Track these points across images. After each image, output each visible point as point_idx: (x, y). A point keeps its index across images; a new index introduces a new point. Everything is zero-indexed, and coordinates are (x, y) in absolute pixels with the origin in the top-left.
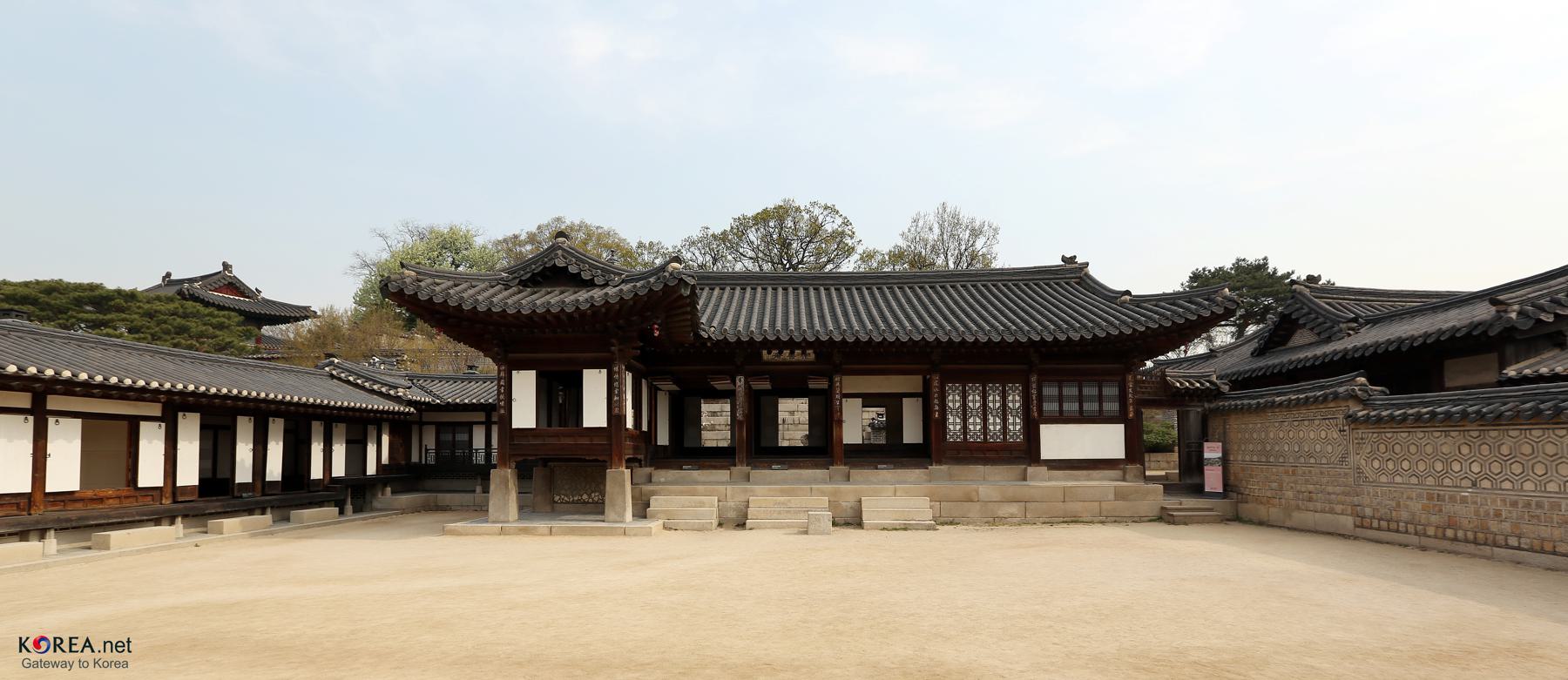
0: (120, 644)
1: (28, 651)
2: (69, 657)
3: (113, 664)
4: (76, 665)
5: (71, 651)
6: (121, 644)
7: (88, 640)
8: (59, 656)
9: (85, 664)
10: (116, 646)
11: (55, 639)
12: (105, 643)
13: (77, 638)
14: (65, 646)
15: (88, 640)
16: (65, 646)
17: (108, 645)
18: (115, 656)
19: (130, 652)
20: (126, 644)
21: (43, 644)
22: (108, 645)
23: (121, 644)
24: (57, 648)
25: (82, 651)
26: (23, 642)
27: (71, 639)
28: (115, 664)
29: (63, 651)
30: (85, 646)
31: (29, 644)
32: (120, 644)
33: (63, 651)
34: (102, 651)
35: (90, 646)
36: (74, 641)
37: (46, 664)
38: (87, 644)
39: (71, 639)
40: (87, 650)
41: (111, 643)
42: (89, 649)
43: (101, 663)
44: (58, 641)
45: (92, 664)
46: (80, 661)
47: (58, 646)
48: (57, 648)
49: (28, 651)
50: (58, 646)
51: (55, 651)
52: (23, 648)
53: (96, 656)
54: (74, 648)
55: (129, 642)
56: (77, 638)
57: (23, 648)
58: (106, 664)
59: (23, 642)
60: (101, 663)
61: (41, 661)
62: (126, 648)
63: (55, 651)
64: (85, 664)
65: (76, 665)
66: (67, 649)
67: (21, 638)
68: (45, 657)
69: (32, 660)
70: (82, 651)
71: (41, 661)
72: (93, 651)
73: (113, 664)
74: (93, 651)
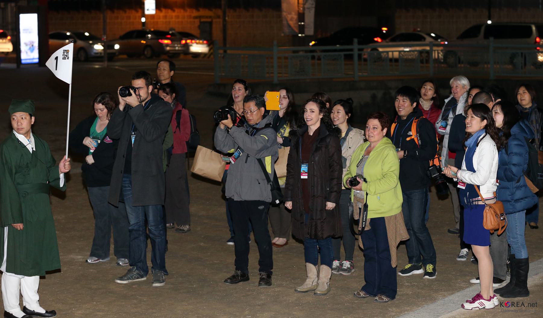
5: (517, 306)
7: (523, 303)
11: (512, 302)
12: (528, 304)
13: (519, 302)
14: (515, 305)
15: (523, 303)
16: (515, 305)
17: (529, 305)
22: (529, 305)
26: (502, 303)
29: (515, 307)
30: (522, 305)
31: (503, 304)
34: (528, 306)
35: (524, 305)
36: (518, 303)
37: (509, 311)
38: (523, 304)
39: (517, 302)
40: (523, 306)
41: (531, 304)
44: (513, 303)
47: (513, 305)
49: (503, 306)
51: (512, 307)
52: (501, 305)
54: (518, 305)
56: (519, 302)
57: (501, 305)
59: (502, 303)
63: (512, 307)
66: (516, 306)
67: (501, 302)
72: (524, 307)
74: (524, 307)
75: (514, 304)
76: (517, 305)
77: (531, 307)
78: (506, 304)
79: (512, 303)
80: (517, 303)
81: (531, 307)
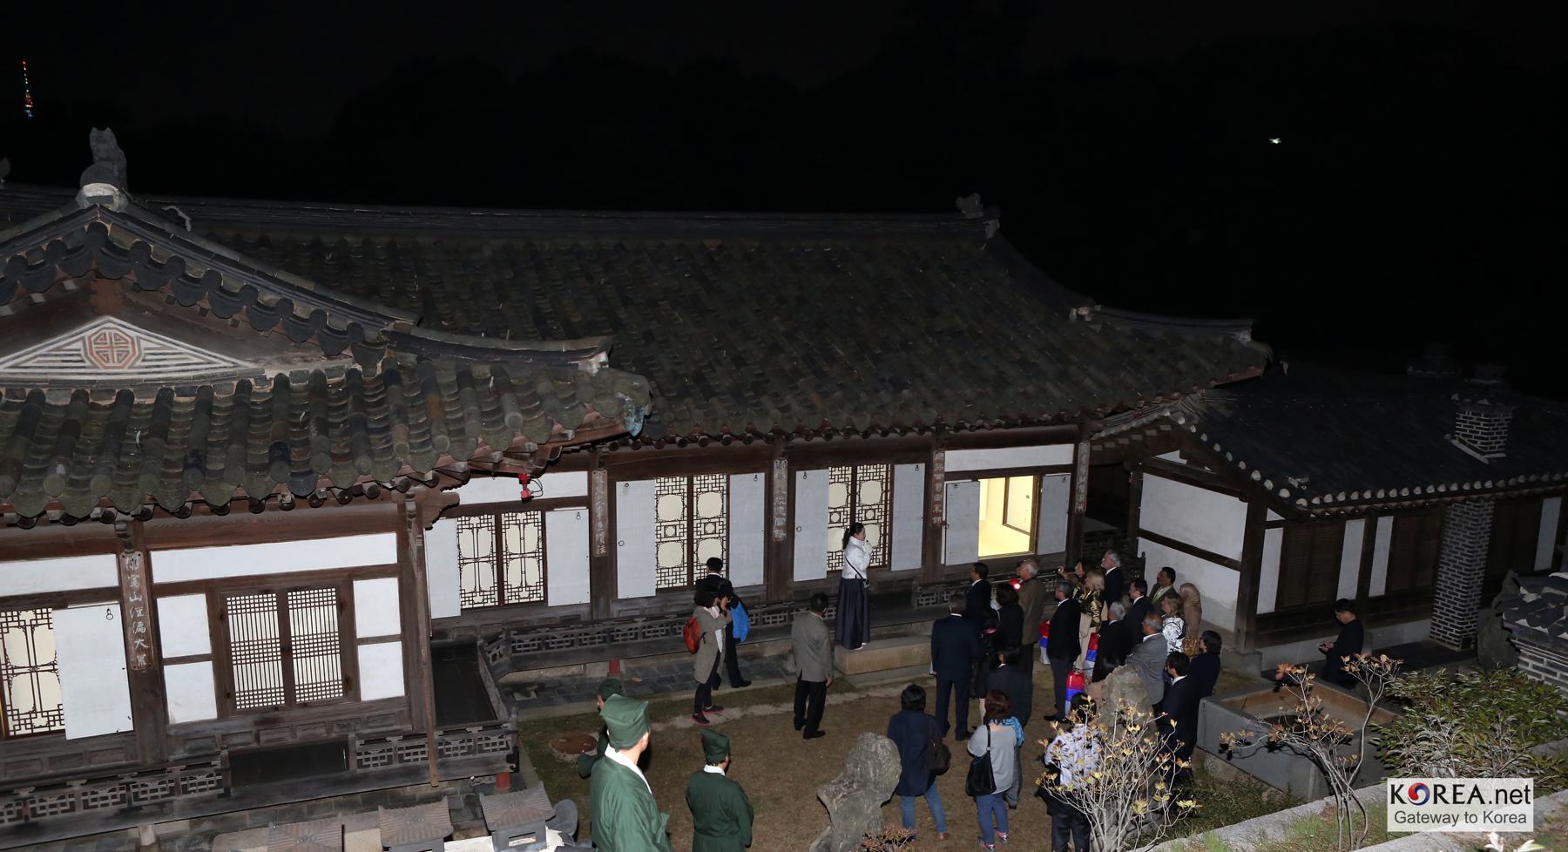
0: (1516, 793)
1: (1402, 802)
2: (1453, 809)
3: (1507, 818)
4: (1462, 817)
5: (1455, 802)
6: (1519, 794)
7: (1476, 789)
8: (1440, 809)
9: (1473, 819)
10: (1511, 796)
11: (1436, 786)
12: (1497, 792)
13: (1463, 786)
14: (1448, 796)
15: (1476, 789)
16: (1448, 796)
17: (1502, 795)
18: (1510, 809)
19: (1529, 803)
20: (1524, 794)
21: (1421, 794)
22: (1502, 795)
23: (1519, 794)
24: (1438, 798)
25: (1469, 802)
26: (1396, 790)
27: (1455, 786)
28: (1510, 819)
29: (1446, 802)
30: (1472, 796)
32: (1516, 793)
33: (1446, 802)
34: (1494, 801)
35: (1479, 796)
36: (1459, 790)
38: (1476, 794)
39: (1455, 786)
40: (1476, 800)
42: (1478, 799)
43: (1492, 816)
44: (1440, 790)
45: (1481, 817)
46: (1466, 815)
47: (1440, 795)
48: (1438, 798)
49: (1402, 802)
50: (1440, 795)
51: (1435, 802)
52: (1396, 798)
53: (1488, 808)
54: (1459, 798)
55: (1527, 790)
56: (1463, 786)
57: (1396, 798)
58: (1498, 819)
59: (1396, 790)
60: (1492, 816)
61: (1418, 815)
62: (1524, 798)
63: (1435, 802)
66: (1450, 800)
68: (1423, 810)
70: (1469, 802)
71: (1418, 815)
72: (1482, 802)
73: (1507, 818)
74: (1482, 802)
76: (1455, 798)
77: (1506, 803)
81: (1506, 803)
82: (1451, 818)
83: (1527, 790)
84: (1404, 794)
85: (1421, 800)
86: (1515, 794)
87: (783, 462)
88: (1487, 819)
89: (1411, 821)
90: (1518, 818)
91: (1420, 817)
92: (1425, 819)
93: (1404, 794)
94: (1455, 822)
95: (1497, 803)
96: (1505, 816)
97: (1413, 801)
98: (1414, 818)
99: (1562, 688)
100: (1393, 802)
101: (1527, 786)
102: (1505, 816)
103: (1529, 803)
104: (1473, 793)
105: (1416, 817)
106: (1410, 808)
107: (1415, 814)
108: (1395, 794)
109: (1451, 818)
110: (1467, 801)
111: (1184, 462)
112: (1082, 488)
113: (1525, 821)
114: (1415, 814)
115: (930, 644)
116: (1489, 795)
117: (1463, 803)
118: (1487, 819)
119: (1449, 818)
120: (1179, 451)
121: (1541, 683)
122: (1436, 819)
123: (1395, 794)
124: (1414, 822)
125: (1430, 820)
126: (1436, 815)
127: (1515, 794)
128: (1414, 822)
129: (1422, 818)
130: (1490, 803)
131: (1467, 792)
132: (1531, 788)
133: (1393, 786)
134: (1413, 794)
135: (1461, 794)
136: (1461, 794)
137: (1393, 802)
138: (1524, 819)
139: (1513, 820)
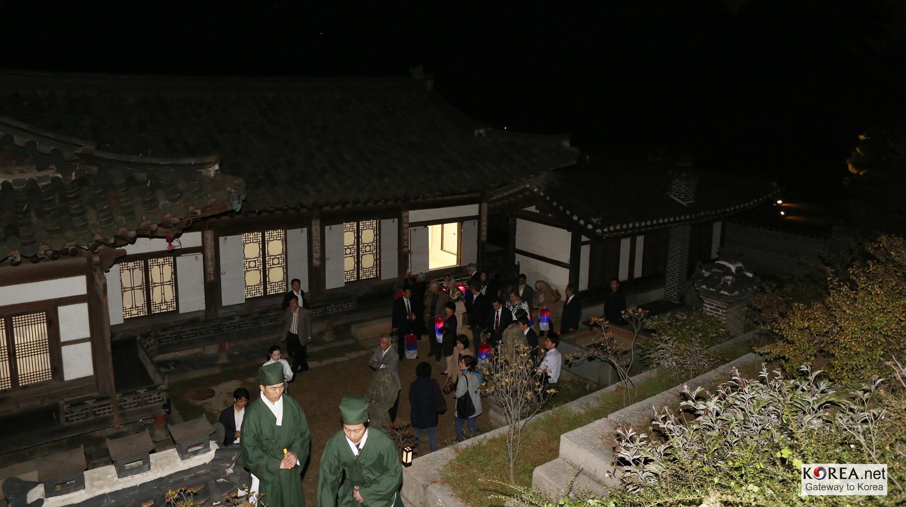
1: (810, 478)
2: (838, 482)
3: (872, 487)
4: (845, 488)
5: (841, 478)
6: (879, 473)
7: (853, 470)
9: (852, 488)
10: (874, 475)
11: (830, 469)
12: (866, 472)
13: (846, 468)
14: (837, 474)
15: (853, 470)
17: (868, 473)
18: (874, 482)
19: (885, 479)
20: (882, 473)
21: (821, 473)
22: (868, 473)
23: (878, 473)
24: (831, 475)
25: (849, 478)
26: (806, 470)
28: (873, 488)
29: (836, 478)
30: (851, 474)
33: (836, 478)
34: (864, 477)
35: (855, 474)
38: (853, 473)
39: (841, 469)
40: (853, 477)
42: (855, 476)
43: (863, 486)
44: (832, 471)
45: (856, 488)
46: (848, 485)
48: (831, 475)
49: (810, 478)
51: (830, 478)
52: (806, 475)
53: (860, 481)
54: (843, 476)
55: (883, 471)
56: (846, 468)
57: (806, 475)
58: (867, 488)
59: (806, 470)
61: (820, 485)
62: (881, 476)
63: (830, 478)
64: (852, 488)
65: (845, 488)
69: (813, 484)
70: (849, 478)
72: (857, 478)
73: (872, 487)
74: (857, 478)
75: (834, 472)
76: (841, 476)
77: (871, 478)
78: (816, 473)
79: (830, 471)
80: (841, 471)
81: (871, 478)
82: (839, 488)
83: (883, 471)
84: (811, 473)
85: (821, 476)
86: (876, 473)
87: (317, 221)
88: (860, 488)
89: (815, 489)
90: (878, 487)
91: (821, 487)
92: (823, 488)
93: (811, 473)
94: (841, 490)
95: (866, 478)
96: (871, 486)
97: (816, 477)
98: (817, 487)
99: (722, 318)
100: (805, 478)
101: (883, 469)
102: (871, 486)
103: (885, 479)
104: (852, 472)
105: (818, 487)
106: (815, 482)
107: (818, 485)
108: (806, 473)
109: (839, 488)
110: (848, 478)
111: (538, 211)
112: (484, 229)
113: (882, 489)
114: (818, 484)
115: (391, 323)
116: (860, 473)
117: (846, 478)
118: (860, 488)
119: (838, 487)
120: (535, 206)
121: (713, 316)
122: (830, 488)
123: (806, 473)
124: (817, 489)
125: (826, 488)
126: (830, 486)
127: (876, 473)
128: (817, 489)
129: (822, 487)
130: (862, 478)
131: (848, 473)
132: (886, 470)
133: (805, 469)
134: (816, 473)
135: (845, 473)
136: (845, 473)
137: (805, 478)
138: (881, 488)
139: (875, 489)
